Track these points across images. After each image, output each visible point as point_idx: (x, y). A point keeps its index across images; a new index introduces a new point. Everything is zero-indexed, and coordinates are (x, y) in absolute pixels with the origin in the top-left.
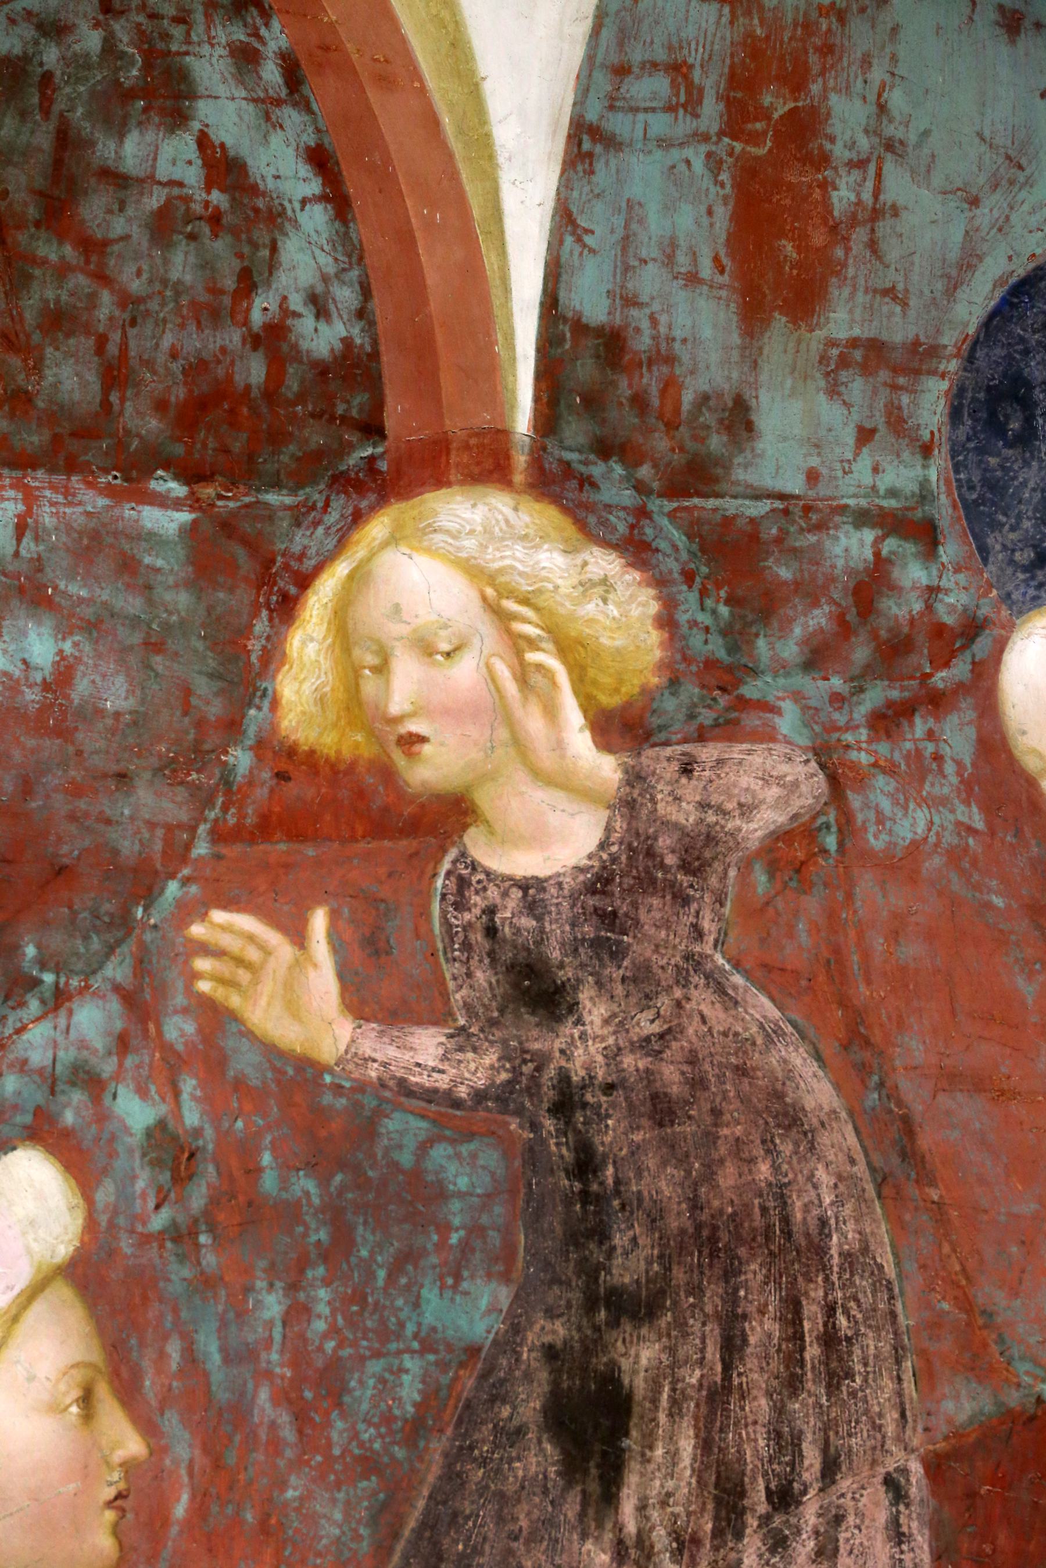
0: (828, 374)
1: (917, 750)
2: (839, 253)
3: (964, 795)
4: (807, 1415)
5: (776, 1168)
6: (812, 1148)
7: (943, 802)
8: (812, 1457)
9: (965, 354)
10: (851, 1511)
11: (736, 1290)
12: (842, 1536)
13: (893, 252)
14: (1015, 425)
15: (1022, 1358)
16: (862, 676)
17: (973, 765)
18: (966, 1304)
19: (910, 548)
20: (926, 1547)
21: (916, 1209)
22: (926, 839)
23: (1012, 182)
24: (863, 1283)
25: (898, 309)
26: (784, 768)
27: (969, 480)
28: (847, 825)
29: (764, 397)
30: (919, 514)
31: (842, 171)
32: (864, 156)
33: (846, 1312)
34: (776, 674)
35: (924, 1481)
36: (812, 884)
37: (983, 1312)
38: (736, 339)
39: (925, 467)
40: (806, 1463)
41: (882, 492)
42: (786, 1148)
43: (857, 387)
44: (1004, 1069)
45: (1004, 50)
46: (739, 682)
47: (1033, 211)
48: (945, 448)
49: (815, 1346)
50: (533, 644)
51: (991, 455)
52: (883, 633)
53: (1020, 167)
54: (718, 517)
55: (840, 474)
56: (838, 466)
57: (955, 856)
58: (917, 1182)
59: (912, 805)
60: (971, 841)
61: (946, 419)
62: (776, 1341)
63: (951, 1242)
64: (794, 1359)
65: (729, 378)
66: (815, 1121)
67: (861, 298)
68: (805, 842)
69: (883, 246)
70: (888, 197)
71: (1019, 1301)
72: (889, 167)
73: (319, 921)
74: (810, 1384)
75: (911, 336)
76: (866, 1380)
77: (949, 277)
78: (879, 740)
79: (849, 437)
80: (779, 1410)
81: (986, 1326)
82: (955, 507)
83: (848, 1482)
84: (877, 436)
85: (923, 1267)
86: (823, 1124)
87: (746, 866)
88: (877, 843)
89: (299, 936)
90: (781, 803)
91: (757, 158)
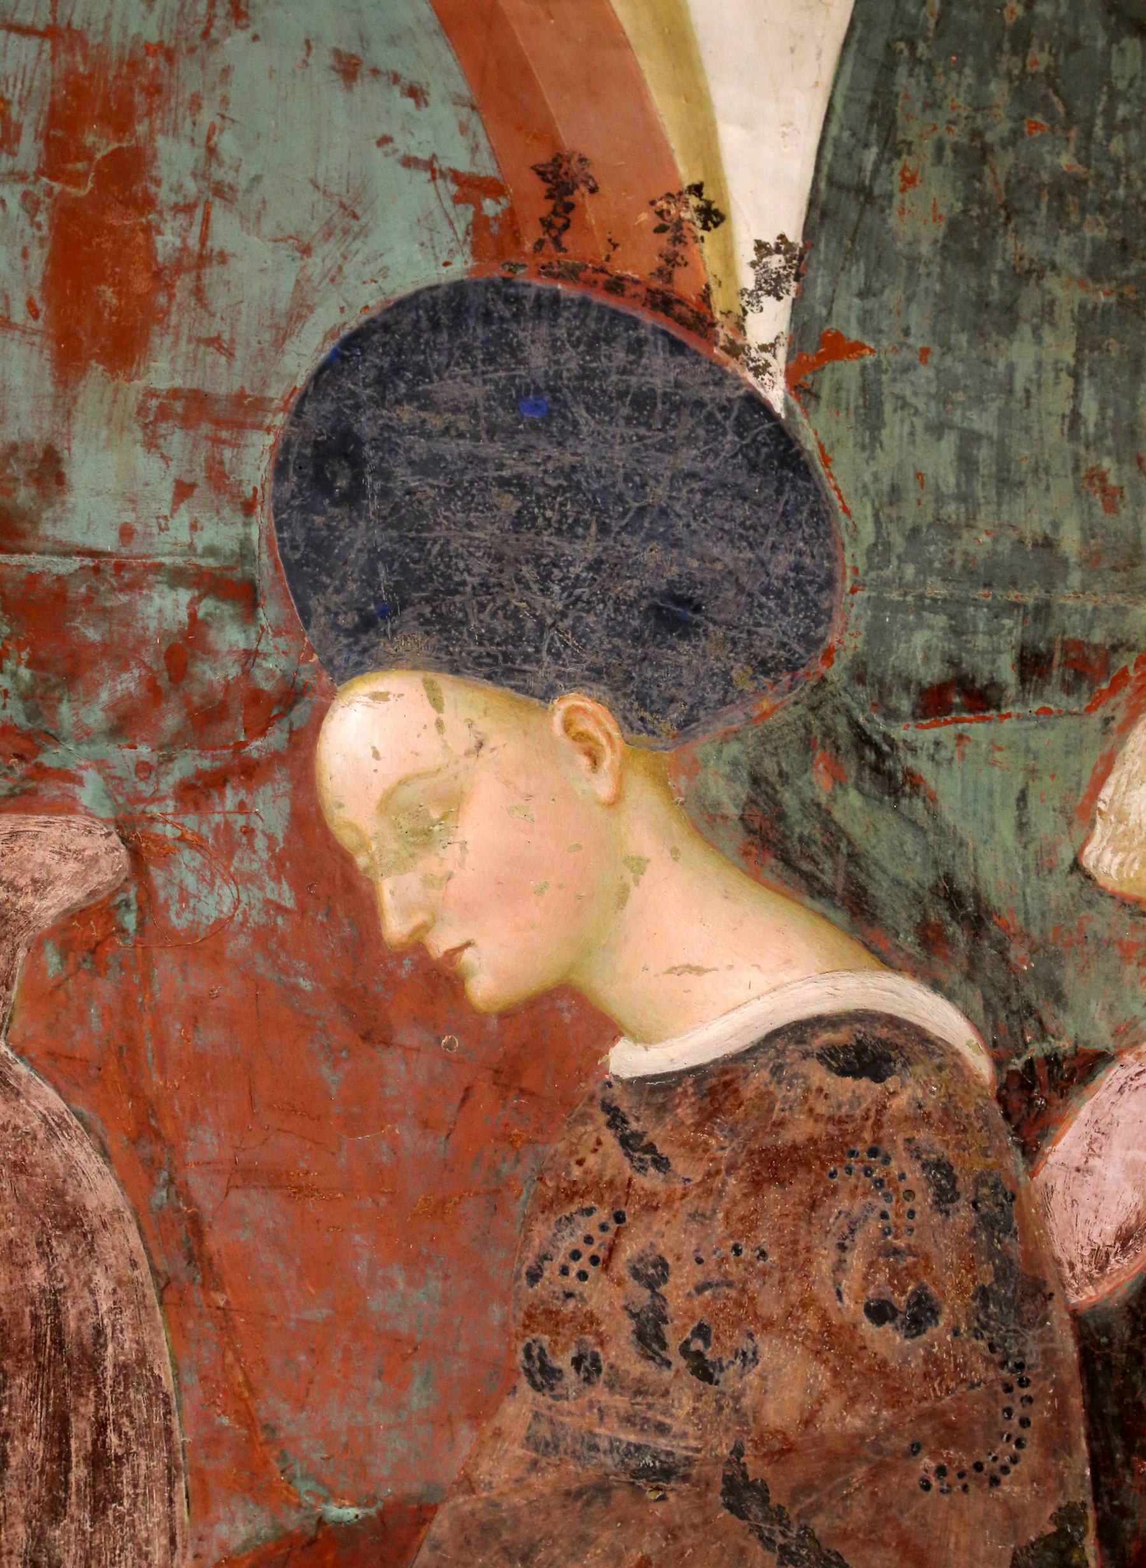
0: (146, 426)
1: (227, 823)
2: (162, 300)
3: (274, 871)
4: (68, 1543)
5: (50, 1273)
6: (91, 1251)
7: (251, 878)
13: (220, 300)
14: (342, 483)
15: (305, 1477)
16: (172, 744)
17: (287, 839)
18: (247, 1418)
19: (227, 609)
21: (200, 1315)
22: (231, 918)
23: (346, 232)
24: (138, 1397)
25: (223, 360)
26: (84, 841)
27: (293, 540)
28: (148, 902)
29: (77, 447)
30: (238, 574)
31: (168, 216)
32: (191, 201)
36: (107, 966)
37: (265, 1427)
38: (48, 386)
39: (246, 525)
41: (199, 551)
42: (63, 1250)
43: (176, 440)
44: (303, 1165)
45: (340, 96)
46: (39, 750)
47: (367, 262)
48: (269, 505)
49: (82, 1467)
51: (317, 513)
52: (196, 699)
53: (355, 217)
54: (23, 575)
55: (155, 530)
56: (153, 522)
57: (262, 936)
58: (203, 1286)
59: (218, 882)
60: (280, 920)
61: (269, 475)
62: (39, 1462)
63: (235, 1351)
64: (58, 1481)
65: (40, 428)
66: (96, 1222)
67: (183, 347)
68: (102, 921)
69: (209, 294)
70: (215, 243)
74: (73, 1508)
75: (236, 388)
77: (278, 328)
78: (186, 813)
79: (166, 492)
80: (38, 1538)
81: (267, 1442)
82: (276, 567)
84: (196, 492)
85: (204, 1379)
86: (104, 1225)
87: (37, 946)
88: (179, 921)
90: (78, 879)
91: (77, 199)
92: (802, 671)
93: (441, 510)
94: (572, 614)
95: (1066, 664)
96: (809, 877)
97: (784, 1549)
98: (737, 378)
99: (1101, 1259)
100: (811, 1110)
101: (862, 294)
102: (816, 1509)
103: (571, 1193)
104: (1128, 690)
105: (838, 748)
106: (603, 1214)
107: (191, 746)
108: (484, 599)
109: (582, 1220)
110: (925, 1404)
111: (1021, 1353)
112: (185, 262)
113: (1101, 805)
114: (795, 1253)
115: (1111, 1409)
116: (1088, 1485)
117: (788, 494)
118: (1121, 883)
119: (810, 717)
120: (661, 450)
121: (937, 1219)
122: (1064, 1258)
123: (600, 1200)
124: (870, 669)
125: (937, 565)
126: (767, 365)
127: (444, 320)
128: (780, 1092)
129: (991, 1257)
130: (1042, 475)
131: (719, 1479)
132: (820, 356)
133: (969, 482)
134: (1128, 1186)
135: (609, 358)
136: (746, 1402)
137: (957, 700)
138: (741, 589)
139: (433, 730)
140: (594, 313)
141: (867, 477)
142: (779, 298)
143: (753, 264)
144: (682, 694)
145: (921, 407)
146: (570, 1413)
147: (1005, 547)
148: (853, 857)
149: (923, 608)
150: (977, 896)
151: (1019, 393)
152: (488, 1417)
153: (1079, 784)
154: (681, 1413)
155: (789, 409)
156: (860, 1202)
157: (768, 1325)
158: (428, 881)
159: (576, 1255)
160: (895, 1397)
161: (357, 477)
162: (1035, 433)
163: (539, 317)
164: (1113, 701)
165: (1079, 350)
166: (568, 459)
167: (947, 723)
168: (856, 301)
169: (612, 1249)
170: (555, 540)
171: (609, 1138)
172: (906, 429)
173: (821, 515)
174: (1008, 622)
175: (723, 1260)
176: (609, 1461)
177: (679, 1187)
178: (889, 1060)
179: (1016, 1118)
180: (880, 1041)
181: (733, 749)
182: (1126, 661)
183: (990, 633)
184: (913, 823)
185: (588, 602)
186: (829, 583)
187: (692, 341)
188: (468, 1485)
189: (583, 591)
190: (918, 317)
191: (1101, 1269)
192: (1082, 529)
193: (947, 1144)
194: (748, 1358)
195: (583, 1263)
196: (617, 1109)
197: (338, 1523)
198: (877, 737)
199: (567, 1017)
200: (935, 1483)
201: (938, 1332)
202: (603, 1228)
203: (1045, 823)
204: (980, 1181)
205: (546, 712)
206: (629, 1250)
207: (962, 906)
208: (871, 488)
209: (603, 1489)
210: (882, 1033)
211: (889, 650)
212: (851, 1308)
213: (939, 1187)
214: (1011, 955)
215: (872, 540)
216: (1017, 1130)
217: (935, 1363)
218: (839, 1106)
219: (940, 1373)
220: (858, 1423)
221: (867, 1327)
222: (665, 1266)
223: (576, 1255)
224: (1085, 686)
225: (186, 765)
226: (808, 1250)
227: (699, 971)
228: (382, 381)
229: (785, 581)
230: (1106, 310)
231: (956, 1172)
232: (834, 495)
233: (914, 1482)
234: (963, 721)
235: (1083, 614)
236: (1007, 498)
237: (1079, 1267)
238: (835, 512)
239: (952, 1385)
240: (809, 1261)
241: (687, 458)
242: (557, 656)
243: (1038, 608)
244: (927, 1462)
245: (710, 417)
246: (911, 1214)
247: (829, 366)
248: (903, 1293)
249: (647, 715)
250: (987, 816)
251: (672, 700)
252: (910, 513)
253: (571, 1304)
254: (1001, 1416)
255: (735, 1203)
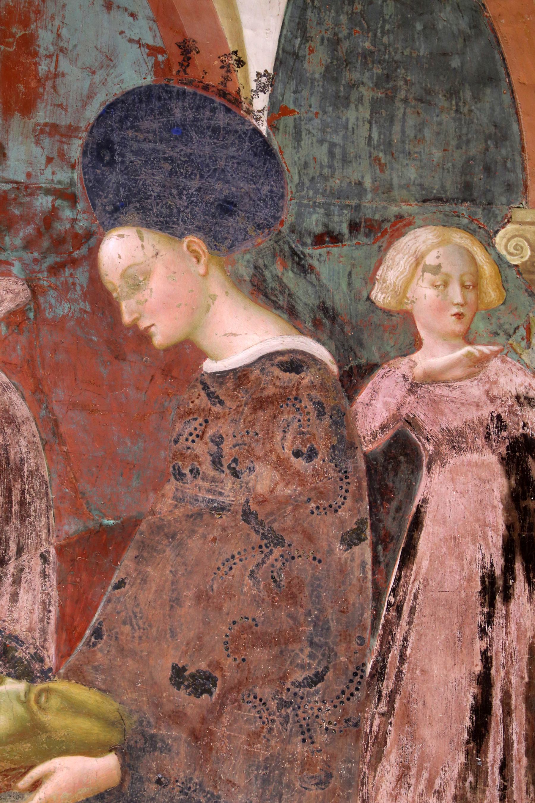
0: (35, 136)
1: (66, 281)
3: (83, 298)
4: (12, 531)
6: (19, 431)
7: (75, 301)
8: (13, 547)
9: (89, 130)
10: (27, 567)
12: (23, 576)
13: (62, 90)
14: (107, 158)
15: (95, 510)
16: (46, 252)
17: (88, 287)
19: (66, 204)
20: (55, 580)
21: (58, 454)
22: (68, 315)
23: (108, 66)
24: (36, 482)
25: (63, 112)
26: (14, 287)
27: (89, 179)
28: (38, 309)
29: (11, 144)
31: (43, 59)
32: (51, 53)
33: (29, 493)
34: (12, 251)
35: (55, 556)
36: (23, 331)
39: (72, 173)
40: (11, 549)
41: (55, 182)
42: (9, 431)
43: (47, 141)
44: (94, 402)
45: (106, 16)
47: (116, 77)
48: (80, 166)
52: (55, 236)
53: (111, 60)
55: (39, 174)
56: (39, 172)
57: (79, 321)
58: (59, 444)
59: (63, 302)
60: (85, 316)
61: (81, 155)
63: (70, 467)
66: (20, 421)
67: (49, 107)
68: (21, 315)
69: (58, 88)
70: (60, 69)
71: (95, 489)
72: (61, 58)
75: (68, 123)
76: (35, 518)
77: (83, 101)
81: (82, 498)
82: (83, 188)
83: (26, 556)
84: (54, 160)
85: (60, 476)
86: (23, 422)
88: (49, 315)
90: (12, 300)
91: (10, 52)
92: (272, 228)
93: (143, 169)
94: (190, 207)
95: (366, 227)
96: (274, 302)
97: (263, 534)
98: (250, 122)
99: (374, 435)
100: (274, 384)
101: (295, 92)
102: (274, 521)
103: (189, 413)
104: (387, 236)
105: (285, 256)
106: (201, 420)
107: (53, 253)
108: (158, 201)
109: (193, 422)
110: (313, 485)
111: (346, 468)
112: (49, 76)
113: (377, 277)
114: (268, 434)
115: (377, 486)
116: (368, 512)
117: (268, 164)
118: (384, 304)
119: (275, 245)
120: (222, 148)
121: (318, 422)
122: (362, 435)
123: (200, 415)
124: (297, 228)
125: (321, 191)
126: (261, 117)
127: (144, 99)
128: (264, 378)
129: (336, 435)
130: (358, 159)
131: (241, 511)
132: (279, 115)
133: (332, 161)
134: (384, 410)
135: (204, 114)
136: (250, 485)
137: (327, 239)
138: (251, 199)
139: (140, 248)
140: (198, 98)
141: (296, 159)
142: (265, 93)
143: (255, 81)
144: (229, 236)
145: (315, 134)
146: (189, 488)
147: (345, 185)
148: (290, 295)
149: (316, 206)
150: (333, 309)
151: (350, 129)
152: (160, 490)
153: (370, 269)
154: (228, 488)
155: (268, 134)
156: (291, 416)
157: (258, 458)
158: (138, 303)
159: (191, 434)
160: (302, 483)
161: (113, 156)
162: (356, 144)
163: (178, 99)
164: (382, 240)
165: (372, 114)
166: (189, 151)
167: (324, 247)
168: (292, 94)
169: (204, 432)
170: (184, 180)
171: (203, 394)
172: (310, 141)
173: (279, 172)
174: (346, 212)
175: (243, 436)
176: (202, 505)
177: (227, 411)
178: (302, 366)
179: (346, 387)
180: (299, 360)
181: (248, 256)
182: (387, 226)
183: (339, 215)
184: (311, 283)
185: (196, 203)
186: (282, 197)
187: (234, 108)
188: (153, 513)
189: (194, 199)
190: (314, 101)
191: (374, 439)
192: (372, 178)
193: (322, 396)
194: (251, 470)
195: (193, 437)
196: (206, 383)
197: (107, 525)
198: (299, 252)
199: (188, 351)
200: (315, 512)
201: (317, 461)
202: (201, 425)
203: (358, 283)
204: (333, 409)
205: (181, 242)
206: (210, 433)
207: (328, 313)
208: (298, 163)
209: (200, 514)
210: (300, 357)
211: (303, 221)
212: (288, 452)
213: (319, 410)
214: (345, 330)
215: (298, 182)
216: (346, 391)
217: (316, 471)
218: (284, 383)
219: (318, 475)
220: (289, 492)
221: (293, 459)
222: (222, 438)
223: (191, 434)
224: (372, 235)
225: (51, 260)
226: (273, 433)
227: (235, 335)
228: (121, 121)
229: (267, 196)
230: (381, 99)
231: (325, 405)
232: (284, 165)
233: (308, 511)
234: (329, 247)
235: (372, 208)
236: (345, 167)
237: (367, 438)
238: (285, 171)
239: (322, 478)
240: (273, 436)
241: (232, 151)
242: (185, 222)
243: (356, 207)
244: (313, 505)
245: (240, 136)
246: (309, 420)
247: (283, 118)
248: (306, 447)
249: (217, 244)
250: (337, 281)
251: (226, 238)
252: (311, 172)
253: (189, 451)
254: (339, 489)
255: (247, 416)
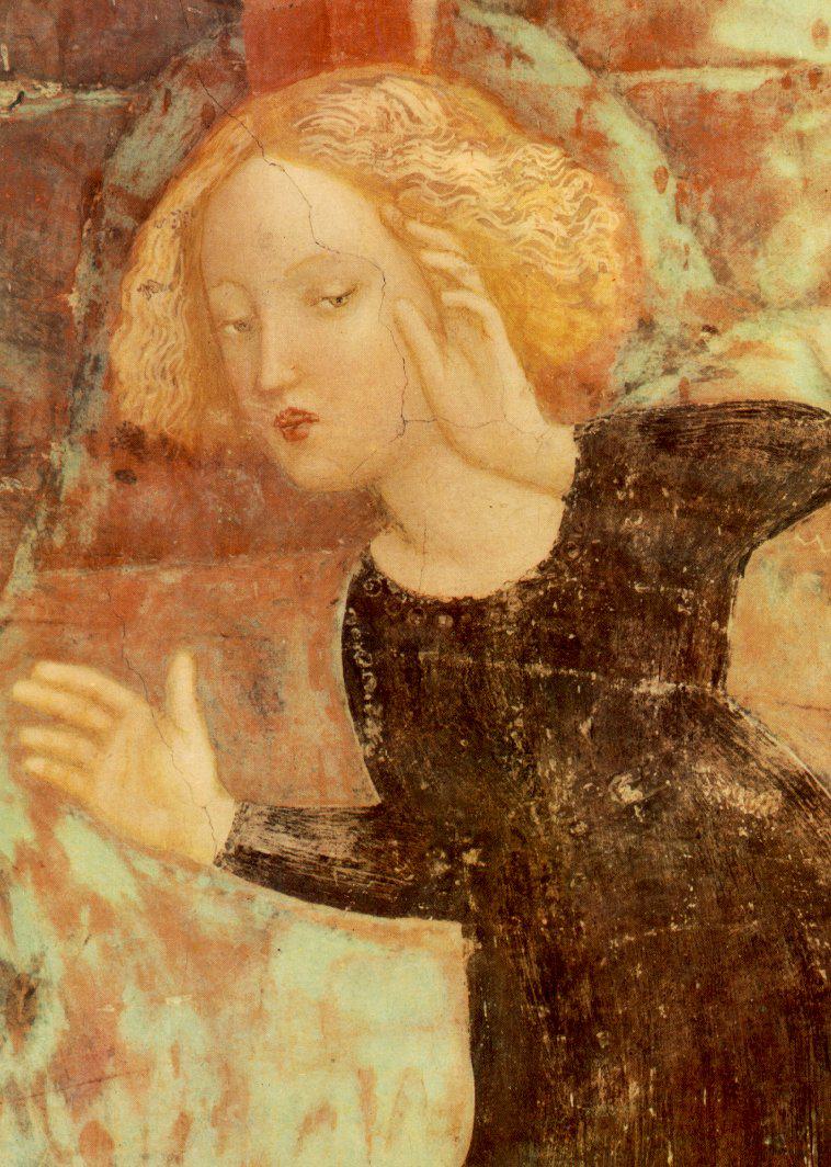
11: (759, 1137)
50: (453, 282)
73: (182, 673)
89: (157, 698)
